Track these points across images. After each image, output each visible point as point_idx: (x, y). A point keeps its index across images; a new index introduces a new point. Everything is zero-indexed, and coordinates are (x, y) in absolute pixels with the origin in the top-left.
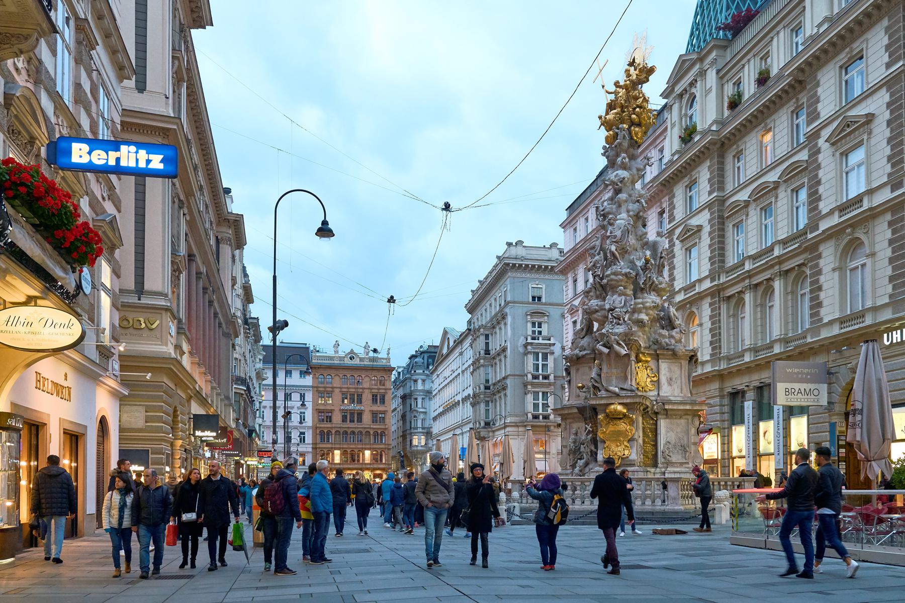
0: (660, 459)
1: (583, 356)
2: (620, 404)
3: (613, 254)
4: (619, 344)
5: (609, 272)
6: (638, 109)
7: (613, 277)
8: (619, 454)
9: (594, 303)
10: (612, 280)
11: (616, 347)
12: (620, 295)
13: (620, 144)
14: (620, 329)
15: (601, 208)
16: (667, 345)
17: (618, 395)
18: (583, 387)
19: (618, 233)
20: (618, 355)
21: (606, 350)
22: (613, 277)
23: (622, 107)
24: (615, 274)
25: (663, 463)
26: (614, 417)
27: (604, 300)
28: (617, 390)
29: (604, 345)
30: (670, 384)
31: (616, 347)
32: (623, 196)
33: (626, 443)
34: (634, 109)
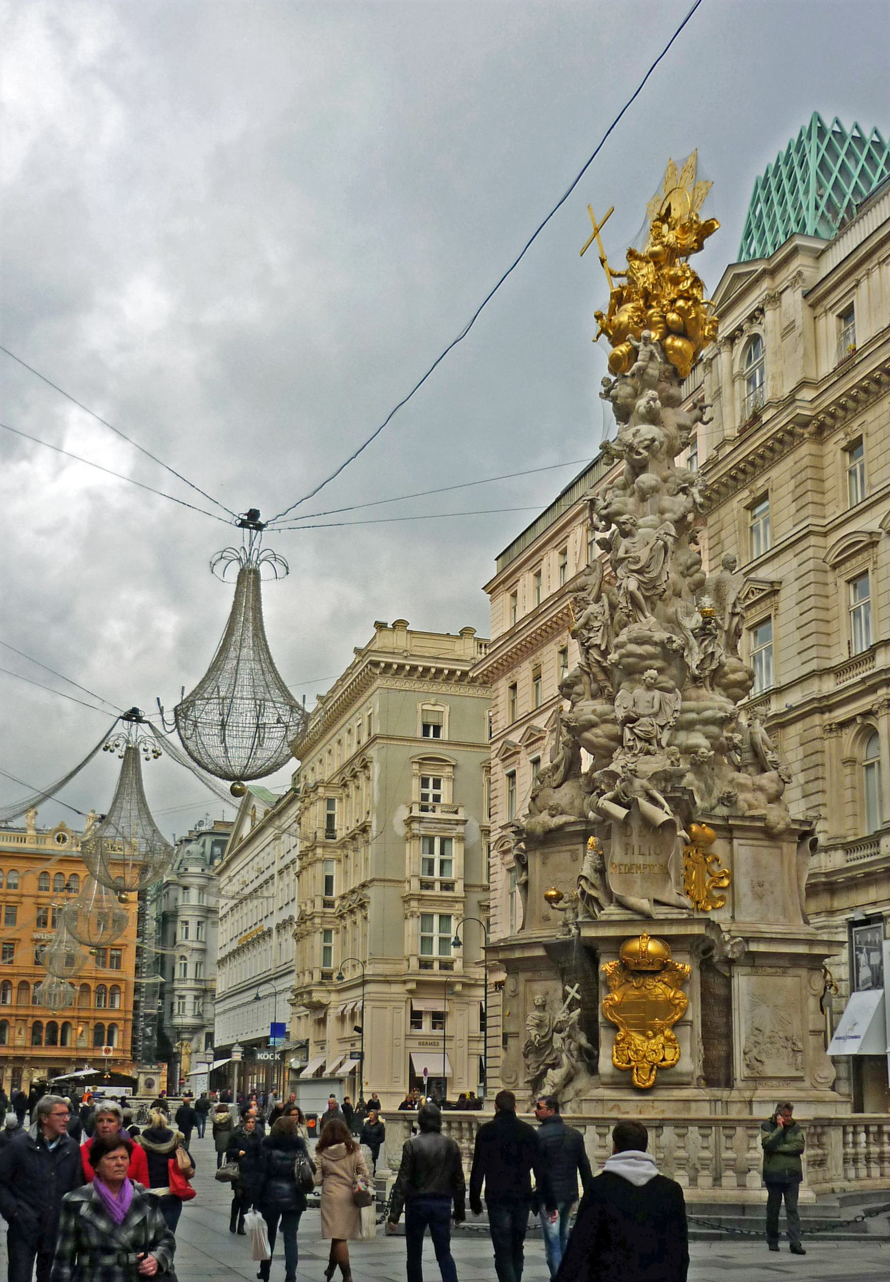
0: (740, 1070)
1: (560, 828)
2: (653, 937)
3: (632, 598)
4: (653, 800)
5: (623, 637)
6: (681, 303)
7: (632, 647)
8: (652, 1057)
9: (589, 708)
10: (630, 655)
11: (645, 805)
12: (649, 688)
13: (642, 371)
14: (658, 763)
15: (601, 503)
16: (751, 807)
17: (647, 919)
18: (559, 898)
19: (644, 554)
20: (647, 822)
21: (621, 812)
22: (632, 647)
23: (647, 296)
24: (640, 641)
25: (746, 1079)
26: (636, 970)
27: (611, 700)
28: (645, 905)
29: (616, 800)
30: (759, 897)
31: (645, 805)
32: (647, 479)
33: (668, 1032)
34: (673, 302)
